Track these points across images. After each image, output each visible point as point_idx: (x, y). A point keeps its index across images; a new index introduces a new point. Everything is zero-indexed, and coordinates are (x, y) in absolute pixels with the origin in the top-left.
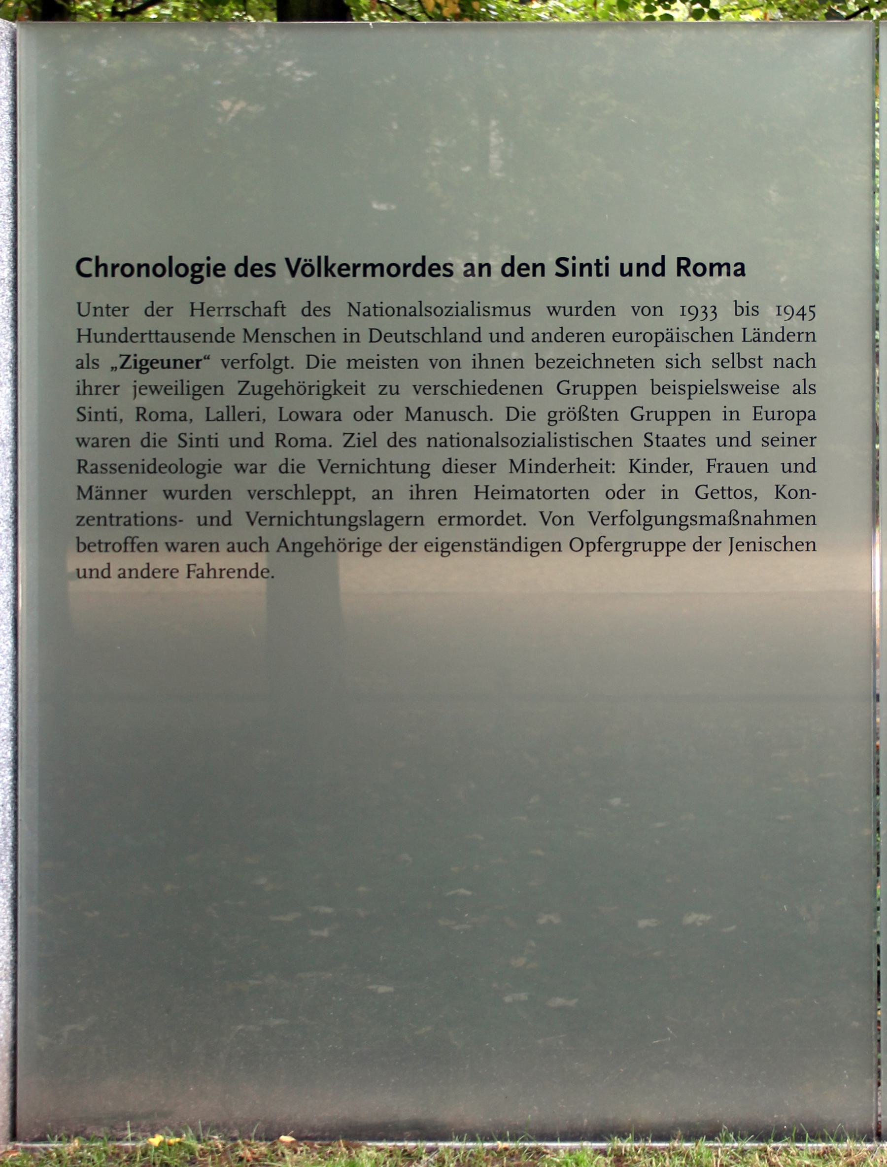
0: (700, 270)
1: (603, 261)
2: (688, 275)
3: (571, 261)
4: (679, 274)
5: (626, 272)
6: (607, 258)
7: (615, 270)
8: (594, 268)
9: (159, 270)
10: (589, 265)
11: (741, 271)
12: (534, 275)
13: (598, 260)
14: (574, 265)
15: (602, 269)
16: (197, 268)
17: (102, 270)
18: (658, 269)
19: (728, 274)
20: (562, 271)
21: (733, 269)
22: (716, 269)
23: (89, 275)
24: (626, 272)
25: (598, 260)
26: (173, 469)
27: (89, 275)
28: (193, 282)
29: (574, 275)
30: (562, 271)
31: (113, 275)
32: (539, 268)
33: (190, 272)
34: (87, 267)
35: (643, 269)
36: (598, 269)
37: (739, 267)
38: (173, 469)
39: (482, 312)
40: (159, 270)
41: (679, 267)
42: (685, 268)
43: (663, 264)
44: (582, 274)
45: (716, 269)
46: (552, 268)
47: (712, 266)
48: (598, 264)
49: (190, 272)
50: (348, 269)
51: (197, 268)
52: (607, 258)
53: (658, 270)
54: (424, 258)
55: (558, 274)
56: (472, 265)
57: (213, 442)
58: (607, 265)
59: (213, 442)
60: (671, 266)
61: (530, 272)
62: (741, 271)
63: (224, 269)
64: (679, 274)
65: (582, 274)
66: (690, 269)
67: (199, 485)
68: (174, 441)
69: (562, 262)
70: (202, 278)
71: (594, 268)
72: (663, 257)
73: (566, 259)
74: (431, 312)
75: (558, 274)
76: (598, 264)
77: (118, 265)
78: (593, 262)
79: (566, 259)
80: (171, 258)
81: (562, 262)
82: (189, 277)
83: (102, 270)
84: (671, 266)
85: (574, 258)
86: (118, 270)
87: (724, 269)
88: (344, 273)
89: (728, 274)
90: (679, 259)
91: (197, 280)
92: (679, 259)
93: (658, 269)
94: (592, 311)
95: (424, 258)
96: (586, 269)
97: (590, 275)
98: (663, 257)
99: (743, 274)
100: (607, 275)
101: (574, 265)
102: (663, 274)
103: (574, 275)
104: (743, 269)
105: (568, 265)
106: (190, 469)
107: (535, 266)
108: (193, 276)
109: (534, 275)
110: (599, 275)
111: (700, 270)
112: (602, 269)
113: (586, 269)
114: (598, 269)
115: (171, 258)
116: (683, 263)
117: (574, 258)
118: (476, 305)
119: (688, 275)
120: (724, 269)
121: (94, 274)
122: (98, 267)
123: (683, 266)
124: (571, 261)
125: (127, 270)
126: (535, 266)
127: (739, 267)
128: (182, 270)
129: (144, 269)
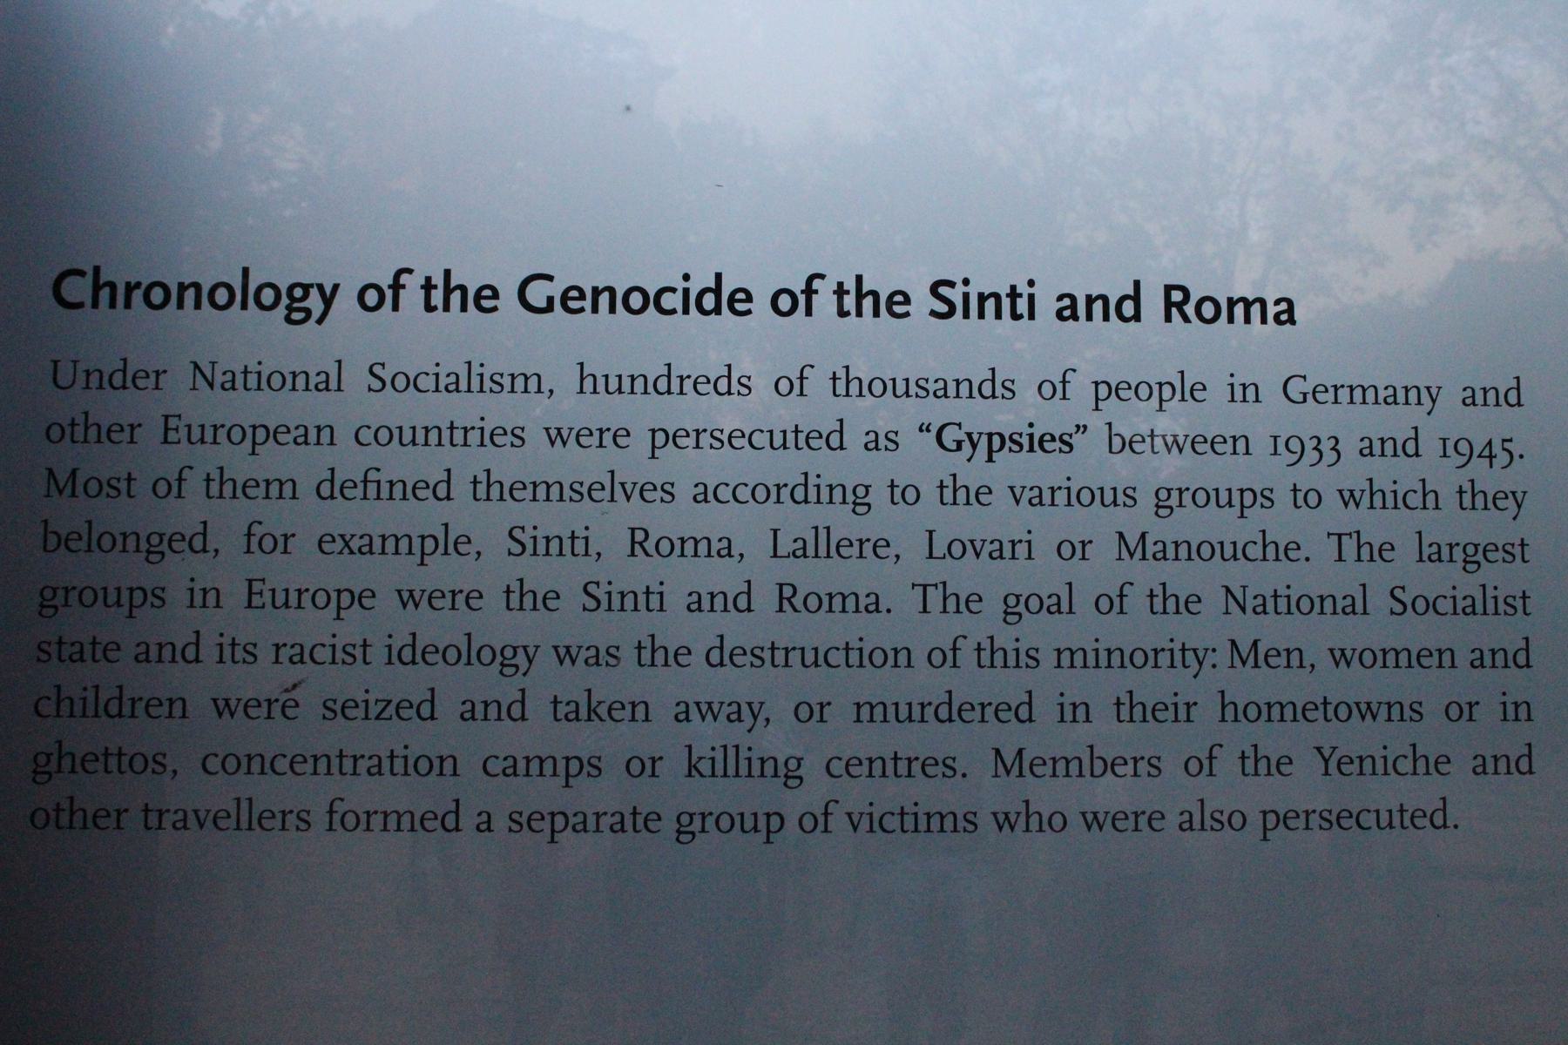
0: (1208, 309)
1: (1023, 289)
2: (1186, 319)
3: (960, 288)
4: (1168, 318)
5: (1068, 310)
6: (1031, 283)
7: (1047, 306)
8: (1006, 303)
9: (222, 296)
10: (997, 296)
11: (1288, 314)
13: (1013, 288)
14: (966, 296)
16: (298, 293)
18: (1127, 307)
19: (1264, 321)
20: (944, 308)
21: (1272, 310)
22: (1239, 310)
23: (80, 305)
24: (1068, 310)
25: (1013, 288)
26: (452, 655)
27: (80, 305)
28: (288, 320)
29: (966, 315)
30: (944, 308)
31: (128, 305)
32: (898, 302)
33: (285, 301)
34: (78, 289)
35: (1098, 307)
37: (1284, 306)
38: (452, 655)
39: (488, 384)
40: (222, 296)
41: (1169, 304)
42: (1180, 306)
43: (1136, 298)
44: (981, 315)
45: (1239, 310)
46: (923, 302)
48: (1014, 294)
49: (285, 301)
50: (582, 297)
51: (298, 293)
52: (1031, 283)
54: (718, 277)
55: (933, 313)
57: (654, 599)
58: (1031, 297)
59: (654, 599)
60: (1153, 303)
64: (1168, 318)
65: (981, 315)
66: (1190, 310)
69: (943, 290)
70: (308, 312)
71: (1006, 303)
72: (1137, 284)
73: (951, 284)
74: (264, 382)
75: (933, 313)
76: (1014, 294)
77: (138, 285)
78: (1004, 291)
79: (951, 284)
80: (246, 271)
81: (943, 290)
82: (281, 311)
84: (1153, 303)
85: (966, 282)
86: (137, 295)
87: (1256, 309)
88: (573, 304)
90: (1168, 289)
91: (297, 316)
92: (1168, 289)
93: (1127, 307)
96: (990, 305)
97: (998, 316)
98: (1137, 284)
99: (1292, 321)
100: (1032, 316)
101: (966, 296)
102: (1137, 317)
103: (966, 315)
104: (1290, 310)
105: (955, 295)
106: (486, 655)
108: (290, 309)
111: (1208, 309)
113: (990, 305)
115: (246, 271)
116: (1177, 296)
117: (966, 282)
118: (476, 369)
119: (1186, 319)
120: (1256, 309)
123: (1176, 301)
124: (960, 288)
125: (157, 295)
127: (1284, 306)
128: (268, 296)
129: (190, 294)
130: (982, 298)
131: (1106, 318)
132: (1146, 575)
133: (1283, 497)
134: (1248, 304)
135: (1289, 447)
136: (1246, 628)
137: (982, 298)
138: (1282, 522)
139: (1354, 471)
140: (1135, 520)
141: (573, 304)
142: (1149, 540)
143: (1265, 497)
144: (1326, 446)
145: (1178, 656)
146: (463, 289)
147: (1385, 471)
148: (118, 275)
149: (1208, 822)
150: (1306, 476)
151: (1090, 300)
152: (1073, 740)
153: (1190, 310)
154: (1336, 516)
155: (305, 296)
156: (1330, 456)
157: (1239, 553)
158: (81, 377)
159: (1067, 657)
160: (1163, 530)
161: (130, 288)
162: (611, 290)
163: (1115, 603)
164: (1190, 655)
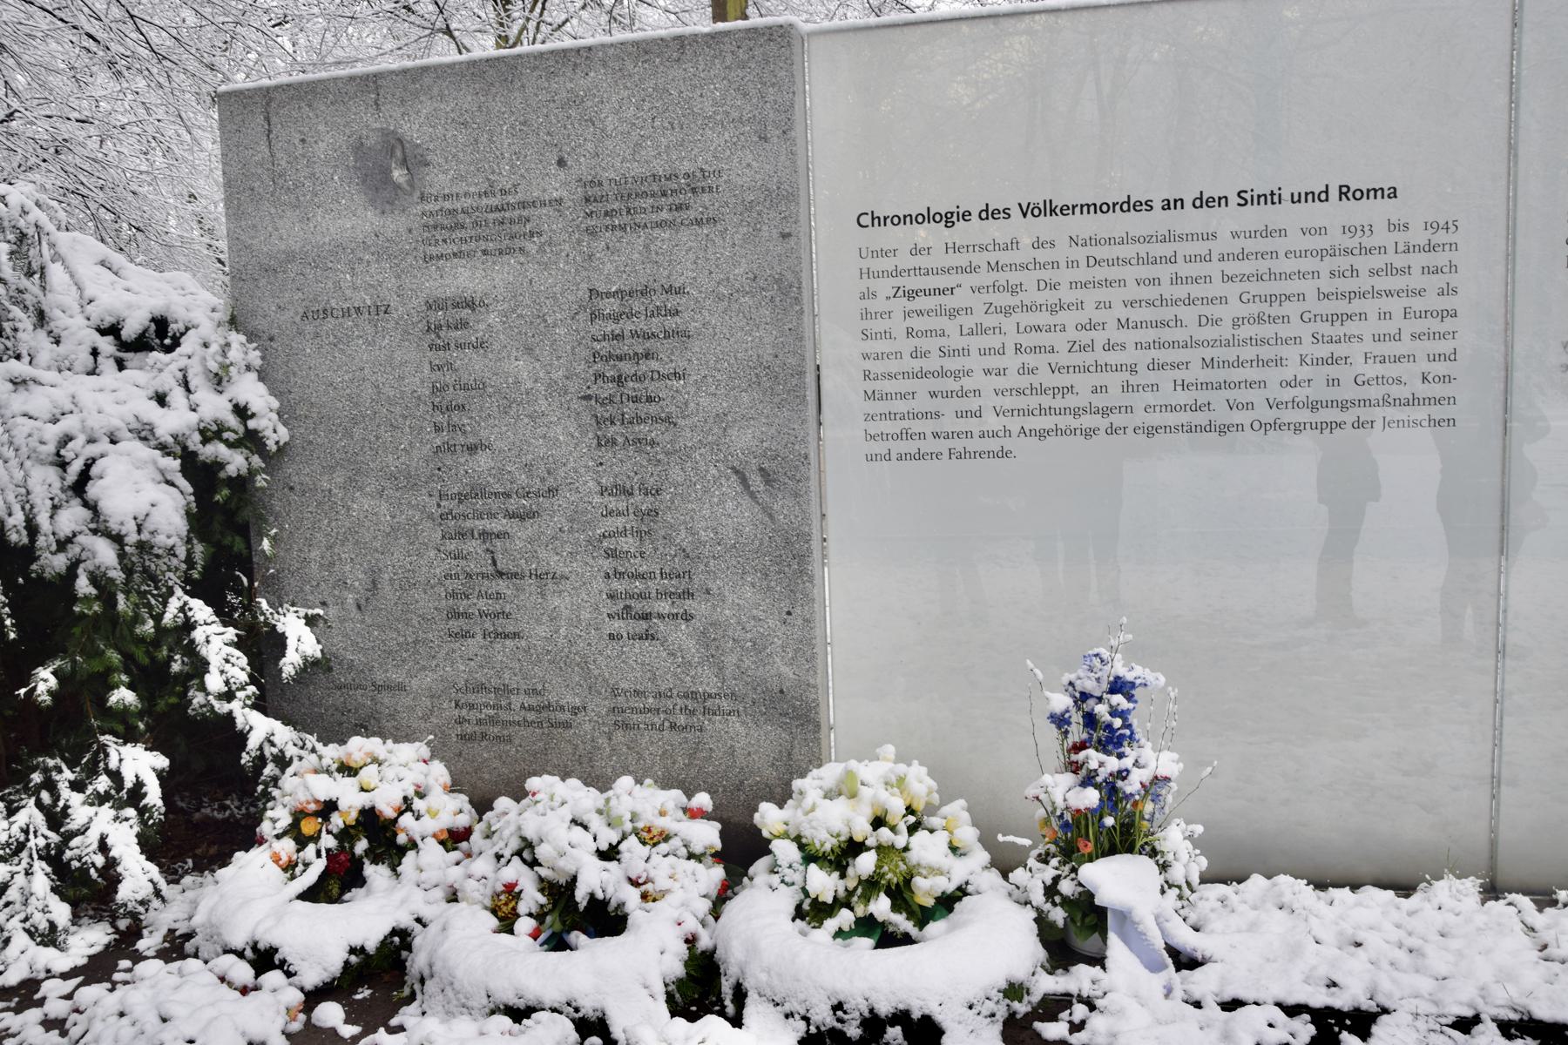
0: (1358, 195)
2: (1348, 199)
3: (1250, 193)
4: (1340, 199)
6: (1280, 189)
8: (1269, 198)
10: (1265, 196)
11: (1394, 194)
12: (1219, 206)
14: (1252, 196)
15: (1276, 199)
17: (876, 221)
19: (1383, 197)
20: (1243, 202)
21: (1386, 193)
22: (1372, 193)
23: (867, 226)
26: (936, 374)
27: (867, 226)
28: (946, 226)
29: (1252, 204)
30: (1243, 202)
33: (944, 219)
35: (1310, 197)
36: (1272, 198)
37: (1392, 190)
38: (936, 374)
39: (1177, 238)
41: (1341, 193)
42: (1345, 194)
43: (1327, 192)
44: (1259, 204)
45: (1372, 193)
46: (1234, 200)
47: (1368, 191)
48: (1272, 194)
50: (1068, 209)
51: (949, 215)
52: (1280, 189)
53: (1323, 196)
54: (1129, 197)
55: (1239, 205)
56: (1168, 201)
57: (966, 352)
58: (1280, 195)
59: (966, 352)
60: (1334, 193)
61: (1216, 204)
62: (1394, 194)
63: (970, 214)
64: (1340, 199)
65: (1259, 204)
66: (1350, 195)
67: (956, 386)
68: (936, 353)
69: (1242, 195)
70: (953, 223)
71: (1269, 198)
72: (1327, 186)
73: (1246, 192)
75: (1239, 205)
76: (1272, 194)
78: (1268, 193)
79: (1246, 192)
80: (928, 209)
81: (1242, 195)
82: (943, 223)
83: (876, 221)
84: (1334, 193)
85: (1252, 190)
86: (888, 221)
87: (1379, 193)
88: (1065, 212)
89: (1383, 197)
90: (1341, 187)
91: (949, 224)
92: (1341, 187)
94: (1267, 233)
95: (1129, 197)
96: (1262, 199)
97: (1266, 203)
98: (1327, 186)
99: (1395, 197)
100: (1280, 203)
101: (1252, 196)
102: (1327, 200)
103: (1252, 204)
104: (1395, 192)
106: (949, 374)
107: (1220, 198)
108: (946, 222)
109: (1219, 206)
110: (1273, 203)
111: (1358, 195)
112: (1276, 199)
113: (1262, 199)
114: (1272, 198)
115: (928, 209)
116: (1344, 190)
117: (1252, 190)
118: (1172, 233)
119: (1348, 199)
120: (1379, 193)
121: (870, 224)
122: (873, 219)
123: (1344, 192)
124: (1250, 193)
126: (1220, 198)
129: (908, 219)
130: (1259, 196)
131: (1313, 201)
137: (1259, 196)
141: (1138, 208)
146: (879, 218)
148: (879, 213)
151: (1176, 201)
153: (1350, 195)
155: (952, 216)
158: (870, 254)
161: (885, 219)
162: (911, 216)
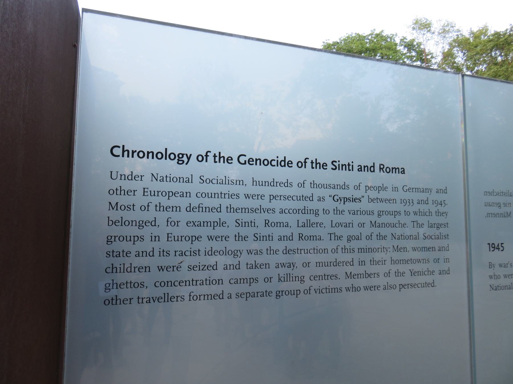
1: (351, 164)
3: (338, 163)
6: (352, 162)
8: (347, 167)
10: (345, 165)
14: (339, 165)
18: (371, 169)
19: (399, 173)
20: (334, 167)
29: (339, 169)
30: (334, 167)
36: (348, 167)
41: (380, 168)
42: (382, 169)
43: (374, 167)
44: (342, 169)
46: (330, 166)
48: (349, 165)
53: (372, 169)
55: (332, 169)
58: (352, 165)
64: (380, 171)
65: (342, 169)
66: (384, 169)
69: (334, 163)
73: (336, 162)
75: (332, 169)
76: (349, 165)
78: (347, 164)
79: (336, 162)
81: (334, 163)
87: (397, 170)
93: (371, 169)
97: (346, 170)
98: (374, 163)
99: (404, 173)
101: (339, 165)
102: (374, 171)
103: (339, 169)
104: (404, 171)
110: (349, 170)
113: (344, 167)
116: (382, 167)
119: (384, 172)
120: (397, 170)
124: (338, 163)
130: (342, 165)
132: (376, 231)
133: (403, 213)
134: (396, 169)
135: (404, 202)
136: (396, 243)
137: (342, 165)
138: (403, 219)
139: (416, 207)
140: (374, 218)
142: (377, 223)
143: (399, 213)
144: (411, 201)
145: (382, 249)
147: (423, 207)
149: (389, 288)
150: (408, 208)
152: (361, 270)
154: (413, 217)
156: (412, 204)
157: (394, 226)
159: (361, 250)
160: (380, 220)
163: (369, 237)
164: (385, 249)
